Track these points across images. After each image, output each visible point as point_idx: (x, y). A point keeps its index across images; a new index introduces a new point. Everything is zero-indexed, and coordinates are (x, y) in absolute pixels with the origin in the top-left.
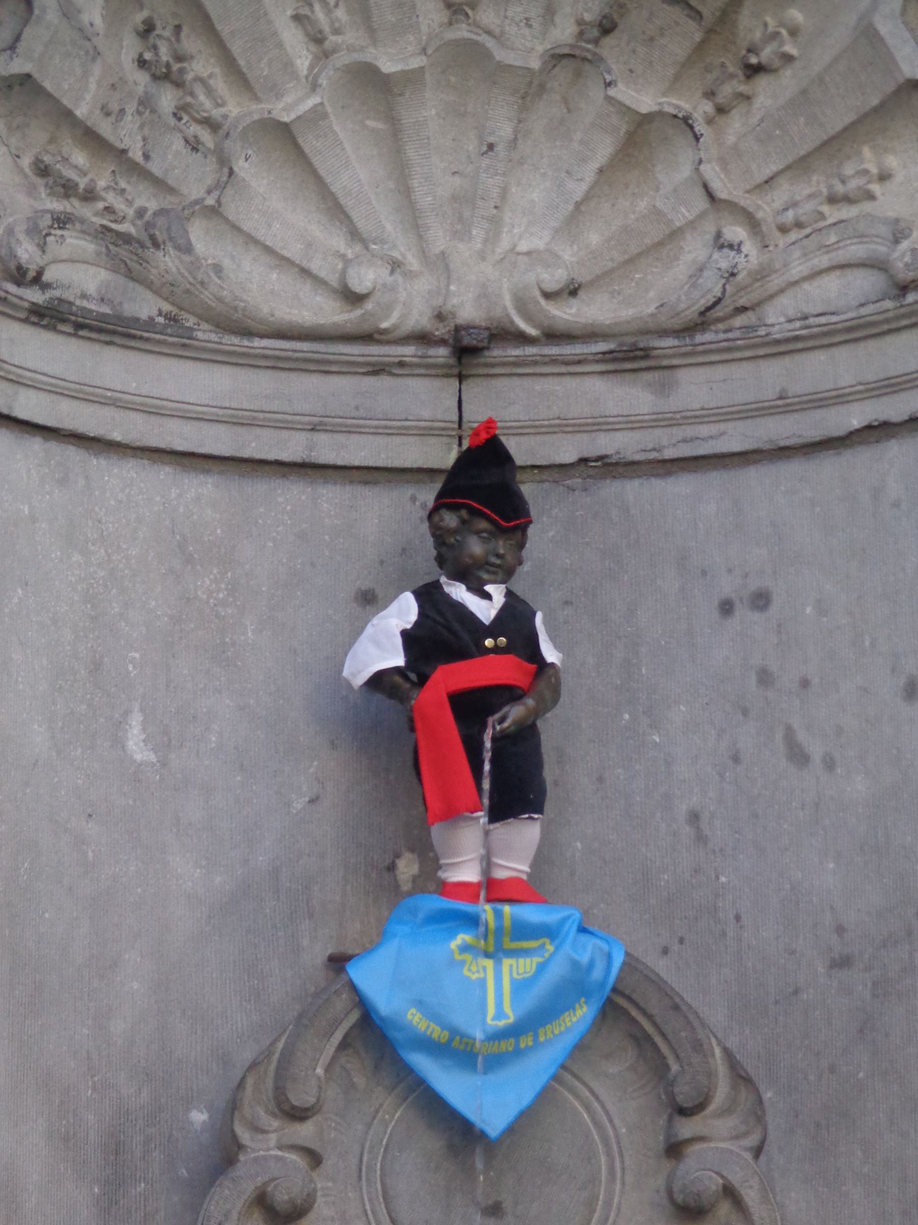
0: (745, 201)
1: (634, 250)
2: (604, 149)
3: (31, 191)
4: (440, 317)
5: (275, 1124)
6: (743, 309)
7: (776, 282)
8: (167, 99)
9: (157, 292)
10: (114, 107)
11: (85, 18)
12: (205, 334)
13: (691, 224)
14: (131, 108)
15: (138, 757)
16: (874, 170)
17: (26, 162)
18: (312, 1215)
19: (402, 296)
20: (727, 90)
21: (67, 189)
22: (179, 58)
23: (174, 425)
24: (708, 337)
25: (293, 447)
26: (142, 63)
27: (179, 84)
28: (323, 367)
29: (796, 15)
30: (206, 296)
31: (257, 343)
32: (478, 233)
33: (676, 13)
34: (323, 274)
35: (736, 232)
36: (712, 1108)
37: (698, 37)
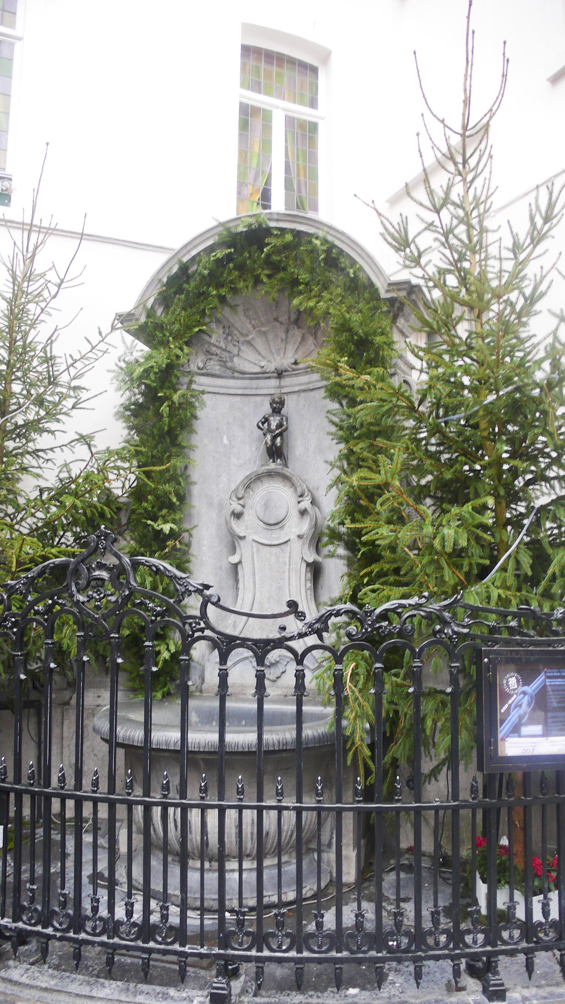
2: (299, 339)
12: (236, 375)
25: (254, 392)
28: (258, 378)
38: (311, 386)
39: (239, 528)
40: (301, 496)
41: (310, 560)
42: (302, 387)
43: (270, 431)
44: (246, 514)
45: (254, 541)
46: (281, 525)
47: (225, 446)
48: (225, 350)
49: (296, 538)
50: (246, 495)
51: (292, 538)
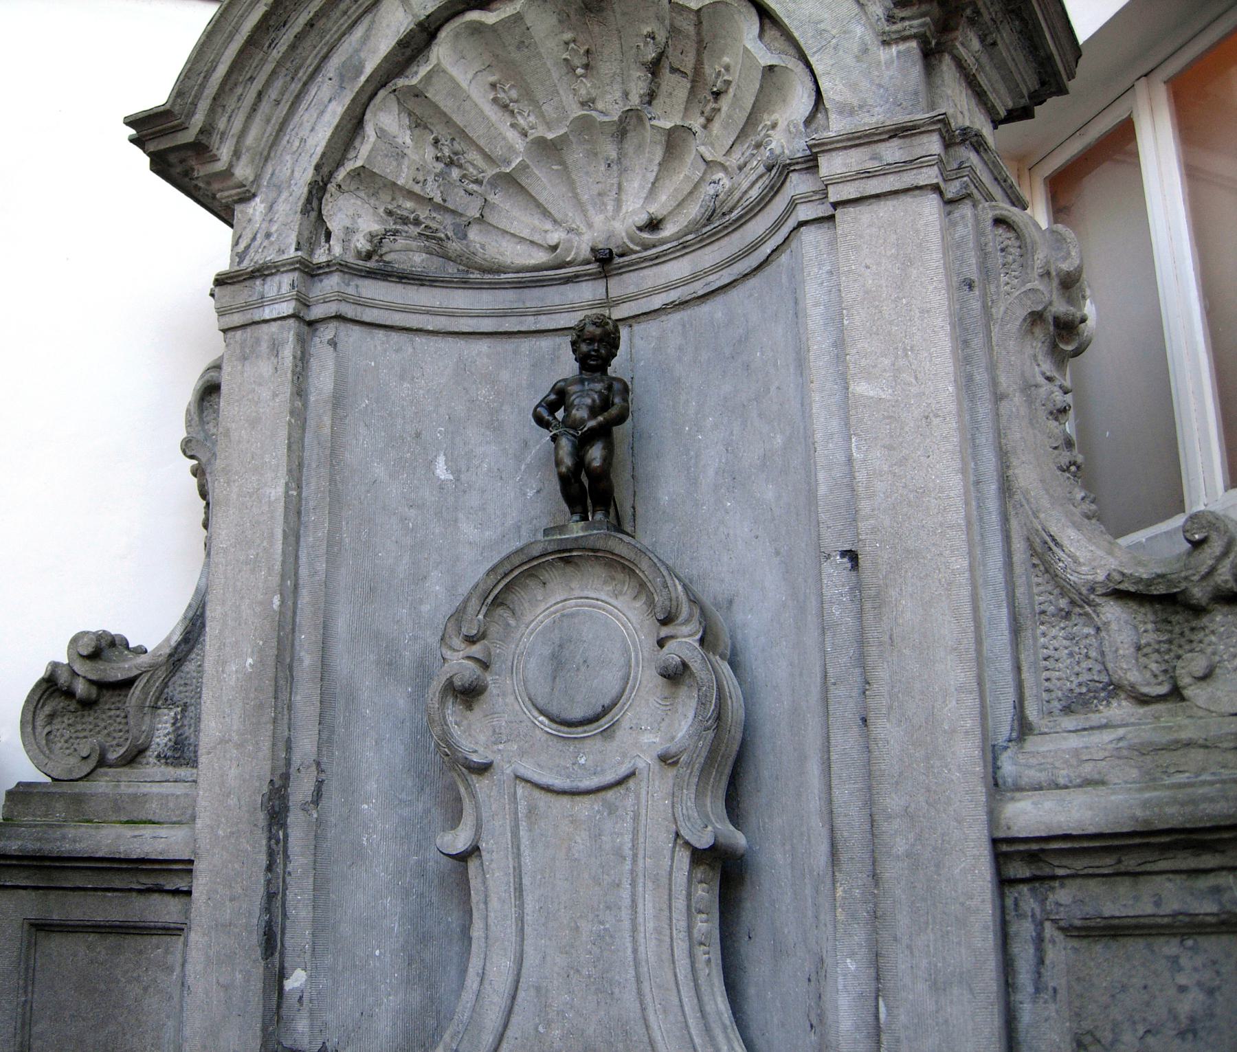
0: (720, 159)
1: (680, 199)
3: (383, 222)
4: (593, 250)
5: (463, 646)
6: (724, 214)
7: (737, 195)
8: (455, 173)
9: (454, 261)
10: (421, 178)
11: (400, 141)
12: (475, 275)
13: (702, 179)
14: (430, 179)
15: (442, 477)
16: (769, 123)
17: (381, 210)
18: (486, 694)
19: (576, 244)
20: (708, 108)
21: (405, 221)
22: (456, 153)
23: (463, 321)
24: (708, 228)
25: (529, 324)
26: (437, 159)
27: (460, 166)
29: (726, 59)
30: (478, 259)
31: (503, 276)
32: (610, 208)
33: (676, 77)
34: (540, 242)
35: (721, 175)
36: (681, 619)
37: (689, 86)
38: (699, 288)
39: (473, 735)
40: (666, 621)
41: (704, 841)
42: (673, 296)
43: (570, 424)
44: (492, 689)
45: (517, 777)
46: (605, 723)
47: (441, 486)
48: (442, 208)
49: (656, 766)
50: (494, 630)
51: (641, 764)
